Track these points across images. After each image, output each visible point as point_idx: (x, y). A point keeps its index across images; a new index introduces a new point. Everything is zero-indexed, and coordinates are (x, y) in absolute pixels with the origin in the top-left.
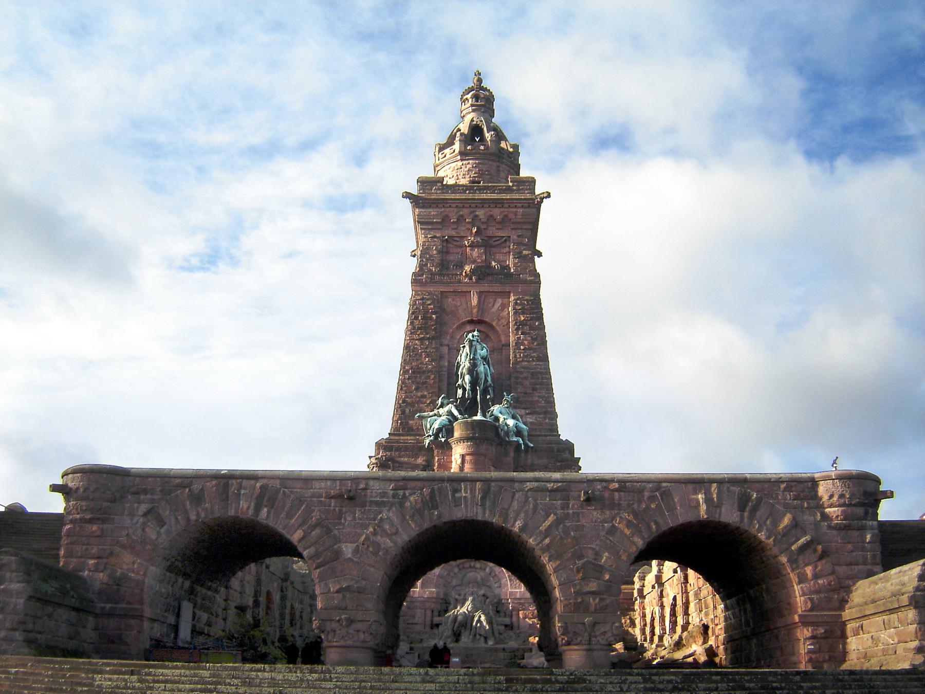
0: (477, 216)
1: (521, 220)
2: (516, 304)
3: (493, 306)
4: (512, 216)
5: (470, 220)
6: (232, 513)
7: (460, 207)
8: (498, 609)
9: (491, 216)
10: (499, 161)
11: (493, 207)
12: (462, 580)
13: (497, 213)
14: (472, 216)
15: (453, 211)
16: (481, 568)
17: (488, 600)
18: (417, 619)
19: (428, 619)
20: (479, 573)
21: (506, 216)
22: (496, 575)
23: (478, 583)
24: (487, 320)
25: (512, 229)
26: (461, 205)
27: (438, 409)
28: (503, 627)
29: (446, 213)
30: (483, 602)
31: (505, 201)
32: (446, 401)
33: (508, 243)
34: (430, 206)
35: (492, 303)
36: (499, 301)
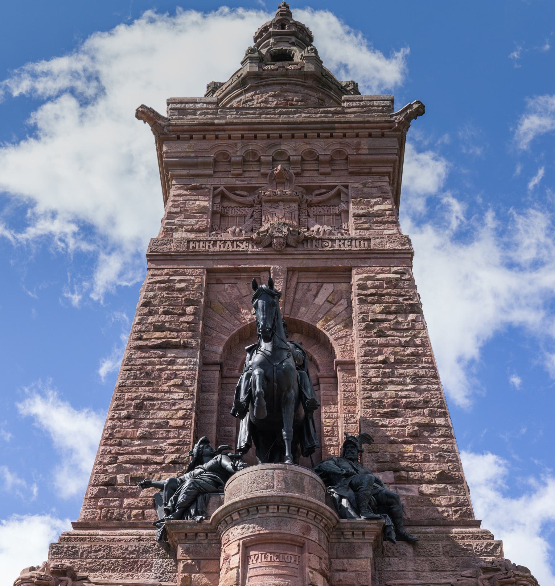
0: (282, 153)
1: (369, 157)
2: (362, 287)
3: (316, 296)
4: (349, 151)
7: (249, 139)
10: (323, 93)
11: (313, 138)
14: (272, 152)
15: (236, 144)
21: (339, 152)
25: (352, 174)
26: (251, 134)
29: (222, 148)
31: (336, 125)
34: (191, 138)
35: (314, 292)
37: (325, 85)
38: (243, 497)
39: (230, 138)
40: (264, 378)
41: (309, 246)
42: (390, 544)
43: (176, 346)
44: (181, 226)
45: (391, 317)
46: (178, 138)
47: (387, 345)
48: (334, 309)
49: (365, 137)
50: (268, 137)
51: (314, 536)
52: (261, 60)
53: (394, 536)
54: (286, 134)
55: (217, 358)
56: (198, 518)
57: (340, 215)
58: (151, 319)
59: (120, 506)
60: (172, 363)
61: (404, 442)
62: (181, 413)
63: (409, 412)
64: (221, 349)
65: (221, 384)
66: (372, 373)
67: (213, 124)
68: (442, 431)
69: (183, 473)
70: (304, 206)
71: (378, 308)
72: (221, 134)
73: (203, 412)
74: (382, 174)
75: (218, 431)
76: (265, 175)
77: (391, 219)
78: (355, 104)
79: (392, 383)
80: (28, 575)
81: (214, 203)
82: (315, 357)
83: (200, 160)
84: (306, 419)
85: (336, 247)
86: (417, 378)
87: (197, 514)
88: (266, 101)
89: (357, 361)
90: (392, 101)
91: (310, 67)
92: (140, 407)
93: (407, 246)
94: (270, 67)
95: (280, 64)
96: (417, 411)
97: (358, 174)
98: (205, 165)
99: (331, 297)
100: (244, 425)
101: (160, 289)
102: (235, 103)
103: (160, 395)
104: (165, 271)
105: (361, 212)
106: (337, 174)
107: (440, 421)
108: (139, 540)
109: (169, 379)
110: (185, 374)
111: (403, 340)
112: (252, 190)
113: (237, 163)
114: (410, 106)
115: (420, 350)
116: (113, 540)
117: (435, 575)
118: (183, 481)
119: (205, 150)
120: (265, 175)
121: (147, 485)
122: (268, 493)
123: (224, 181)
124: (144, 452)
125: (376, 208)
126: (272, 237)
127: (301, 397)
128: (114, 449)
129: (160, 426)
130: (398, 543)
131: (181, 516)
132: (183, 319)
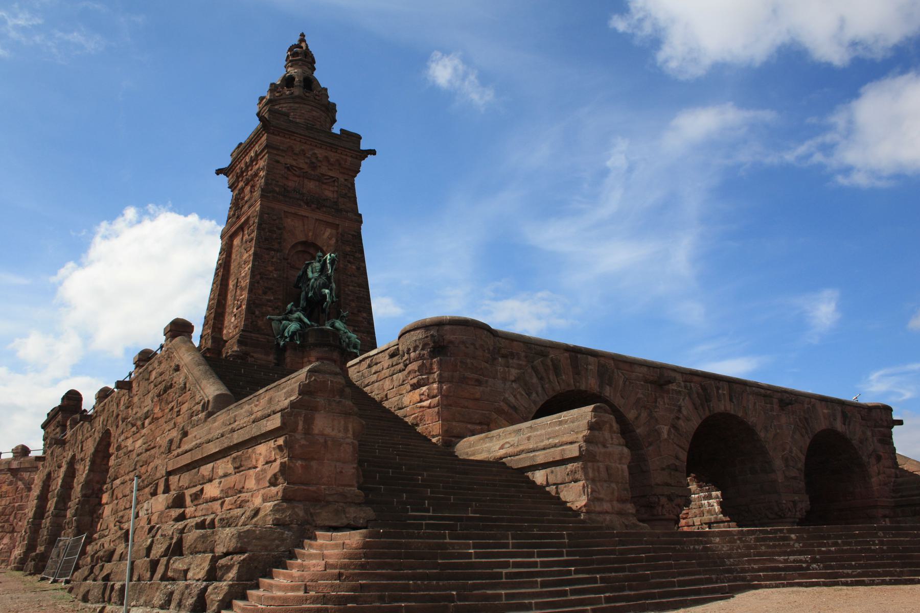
0: (315, 154)
3: (324, 234)
5: (309, 156)
6: (583, 387)
9: (326, 157)
13: (333, 157)
21: (337, 160)
25: (341, 173)
26: (304, 141)
27: (287, 314)
31: (340, 148)
32: (294, 309)
33: (336, 184)
36: (328, 232)
39: (295, 140)
48: (330, 242)
50: (311, 144)
57: (333, 192)
60: (273, 258)
64: (287, 252)
71: (348, 249)
76: (306, 163)
94: (307, 94)
97: (344, 173)
98: (282, 150)
99: (329, 237)
109: (272, 266)
112: (301, 169)
113: (295, 154)
120: (306, 163)
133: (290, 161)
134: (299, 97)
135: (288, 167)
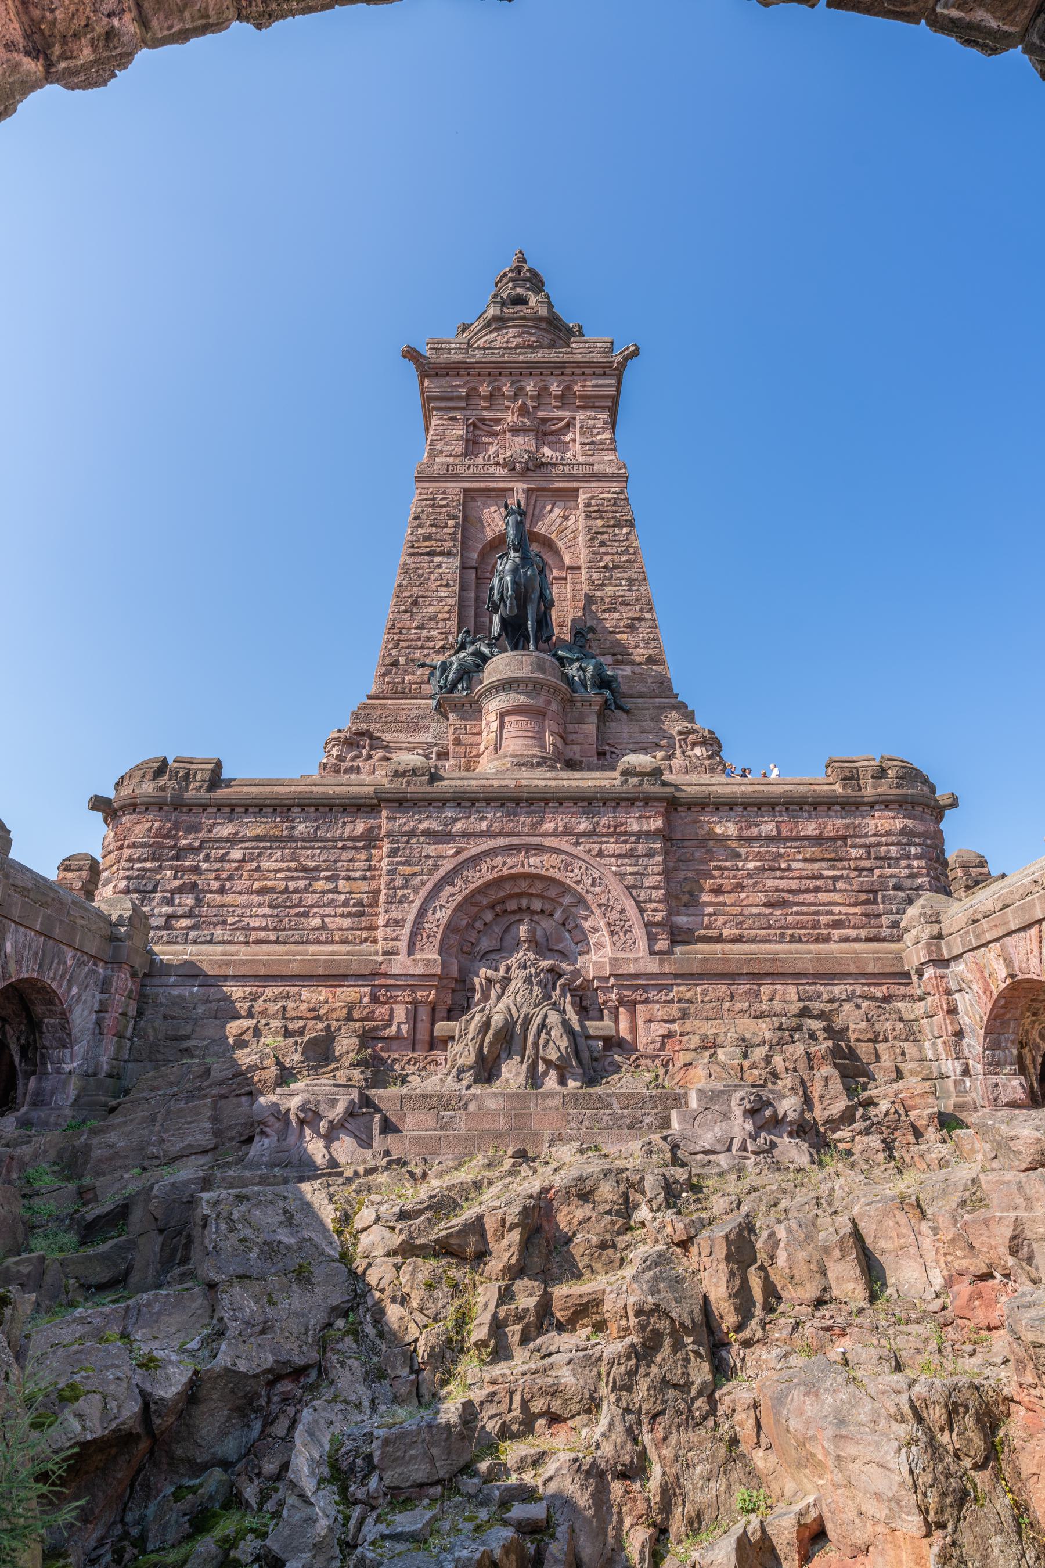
2: (588, 505)
8: (584, 1004)
12: (501, 940)
16: (543, 911)
17: (562, 981)
18: (394, 1028)
19: (423, 1026)
20: (537, 923)
22: (576, 926)
23: (537, 944)
24: (542, 532)
26: (496, 372)
28: (601, 1044)
29: (473, 384)
30: (550, 986)
34: (448, 374)
37: (556, 327)
38: (499, 677)
39: (479, 375)
40: (515, 583)
41: (544, 470)
42: (610, 712)
43: (441, 554)
44: (441, 452)
45: (610, 530)
46: (437, 374)
47: (607, 554)
49: (589, 375)
51: (554, 707)
52: (503, 304)
53: (613, 707)
54: (525, 372)
55: (474, 564)
56: (465, 693)
58: (420, 531)
59: (403, 682)
60: (439, 566)
61: (620, 632)
62: (446, 608)
63: (623, 608)
64: (476, 556)
65: (477, 584)
66: (595, 576)
67: (466, 363)
68: (649, 623)
69: (450, 656)
70: (540, 435)
71: (600, 523)
72: (472, 372)
73: (463, 607)
74: (603, 408)
75: (475, 623)
77: (610, 447)
78: (582, 345)
79: (610, 584)
80: (336, 735)
81: (467, 432)
82: (550, 562)
83: (455, 394)
84: (545, 613)
85: (566, 471)
86: (631, 581)
87: (463, 689)
88: (507, 342)
89: (583, 566)
90: (612, 343)
91: (543, 311)
92: (415, 603)
93: (623, 471)
94: (511, 311)
95: (518, 308)
96: (629, 607)
98: (460, 398)
100: (496, 619)
101: (426, 505)
102: (481, 343)
103: (430, 594)
104: (430, 490)
105: (586, 441)
106: (566, 406)
107: (648, 616)
108: (419, 708)
110: (449, 576)
111: (620, 549)
113: (484, 398)
114: (628, 348)
115: (633, 558)
116: (399, 709)
117: (644, 736)
118: (451, 664)
119: (459, 386)
121: (423, 665)
122: (519, 674)
123: (475, 413)
124: (419, 639)
125: (599, 437)
126: (514, 462)
127: (542, 597)
128: (396, 637)
129: (431, 619)
130: (616, 711)
131: (451, 691)
132: (445, 530)
133: (473, 414)
134: (495, 319)
135: (474, 425)
